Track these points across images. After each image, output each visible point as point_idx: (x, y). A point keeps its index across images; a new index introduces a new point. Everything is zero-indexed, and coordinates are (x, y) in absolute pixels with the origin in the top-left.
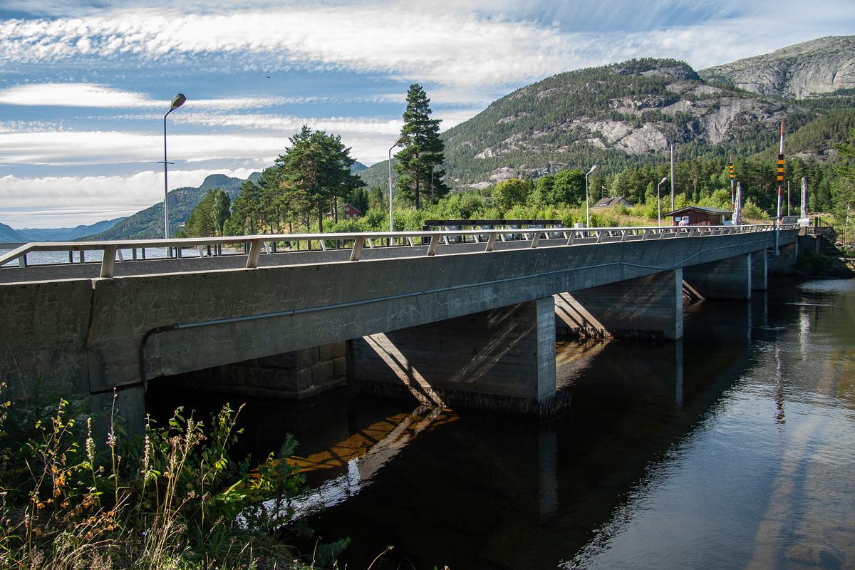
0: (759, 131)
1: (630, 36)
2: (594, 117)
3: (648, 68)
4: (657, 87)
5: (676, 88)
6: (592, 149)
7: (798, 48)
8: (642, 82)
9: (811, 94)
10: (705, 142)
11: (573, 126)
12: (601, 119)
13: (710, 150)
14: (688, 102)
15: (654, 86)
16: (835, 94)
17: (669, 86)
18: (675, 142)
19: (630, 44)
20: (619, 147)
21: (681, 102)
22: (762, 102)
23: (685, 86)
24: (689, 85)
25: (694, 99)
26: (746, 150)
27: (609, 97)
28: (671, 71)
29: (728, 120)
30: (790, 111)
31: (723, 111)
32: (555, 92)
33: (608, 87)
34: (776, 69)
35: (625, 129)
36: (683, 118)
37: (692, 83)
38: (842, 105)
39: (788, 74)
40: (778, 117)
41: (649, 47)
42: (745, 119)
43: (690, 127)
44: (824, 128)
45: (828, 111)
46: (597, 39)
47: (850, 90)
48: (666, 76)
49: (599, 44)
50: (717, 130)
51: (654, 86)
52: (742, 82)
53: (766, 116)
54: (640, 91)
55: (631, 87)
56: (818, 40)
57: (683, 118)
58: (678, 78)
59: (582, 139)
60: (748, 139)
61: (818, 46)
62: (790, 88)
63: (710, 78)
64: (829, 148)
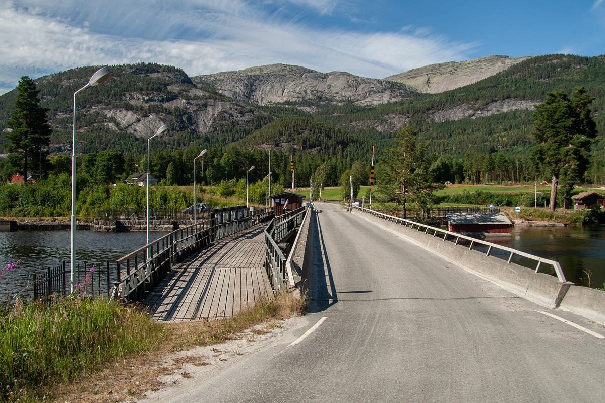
0: (234, 126)
1: (147, 42)
2: (110, 106)
3: (153, 71)
4: (161, 86)
5: (175, 89)
6: (108, 131)
7: (260, 69)
8: (149, 81)
9: (268, 102)
10: (196, 131)
11: (92, 112)
12: (116, 107)
13: (199, 138)
14: (184, 101)
15: (158, 85)
16: (284, 103)
17: (170, 87)
18: (173, 130)
19: (145, 49)
20: (130, 131)
21: (178, 100)
22: (237, 105)
23: (182, 88)
24: (184, 87)
25: (188, 98)
26: (225, 139)
27: (122, 91)
28: (171, 75)
29: (213, 116)
30: (256, 113)
31: (210, 109)
32: (77, 82)
33: (122, 82)
34: (246, 82)
35: (135, 117)
36: (180, 112)
37: (187, 86)
38: (289, 112)
39: (253, 87)
40: (248, 117)
41: (161, 53)
42: (225, 117)
43: (185, 119)
44: (279, 128)
45: (280, 116)
46: (120, 42)
47: (293, 102)
48: (167, 79)
49: (121, 45)
50: (205, 123)
51: (158, 85)
52: (222, 89)
53: (239, 115)
54: (147, 89)
55: (140, 84)
56: (273, 65)
57: (180, 112)
58: (177, 81)
59: (99, 122)
60: (227, 131)
61: (274, 69)
62: (254, 97)
63: (199, 83)
64: (283, 142)
